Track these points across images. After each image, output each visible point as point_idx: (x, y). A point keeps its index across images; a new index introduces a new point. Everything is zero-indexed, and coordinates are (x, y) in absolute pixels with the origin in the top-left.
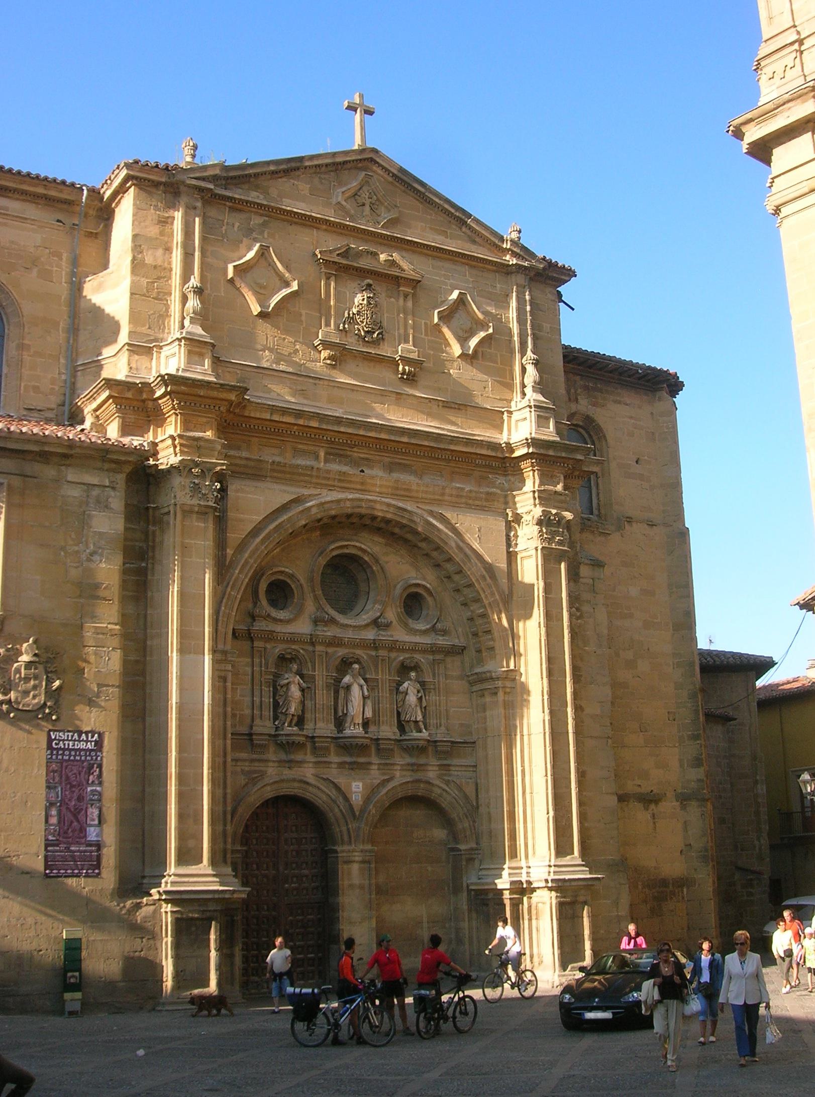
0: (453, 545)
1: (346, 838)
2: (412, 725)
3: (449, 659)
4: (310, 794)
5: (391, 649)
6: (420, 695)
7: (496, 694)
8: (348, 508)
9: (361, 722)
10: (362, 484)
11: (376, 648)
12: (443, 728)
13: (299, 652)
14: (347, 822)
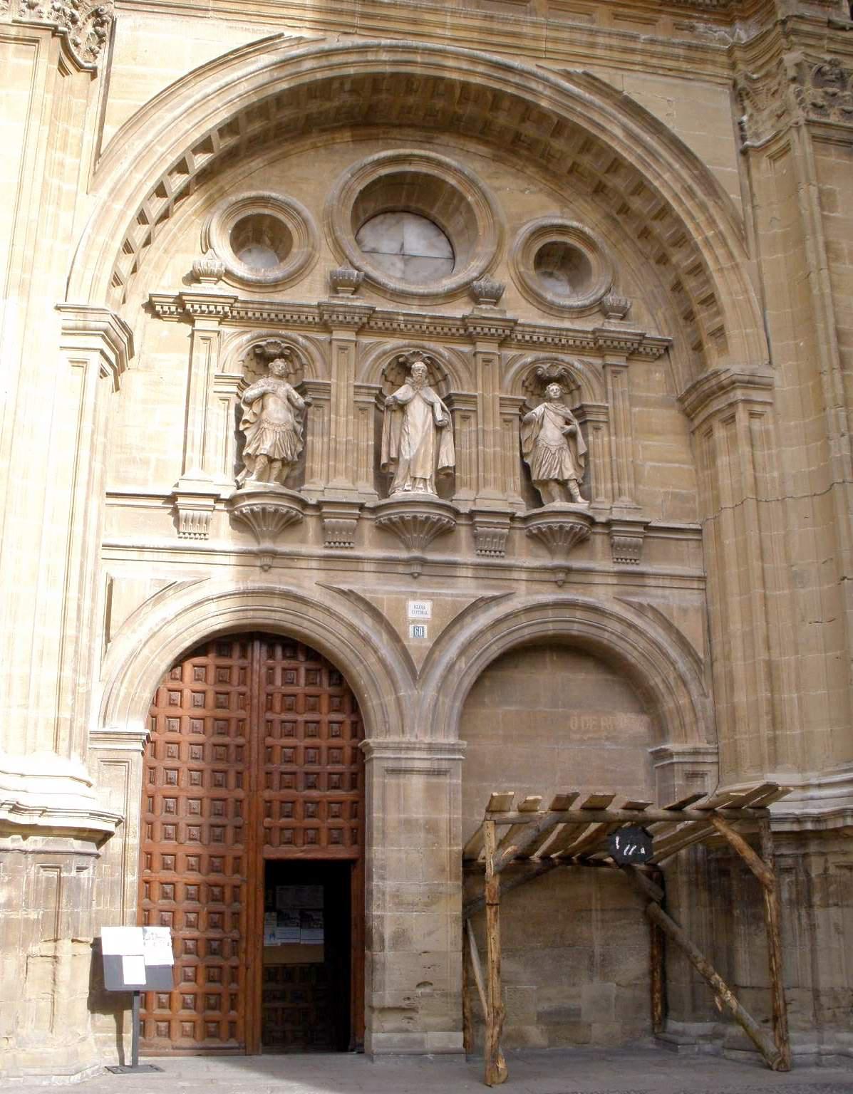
0: (619, 132)
1: (393, 719)
2: (555, 489)
3: (638, 368)
4: (309, 625)
5: (504, 342)
6: (568, 428)
7: (733, 417)
8: (383, 63)
9: (428, 471)
10: (415, 22)
11: (471, 339)
12: (625, 500)
13: (296, 341)
14: (393, 683)
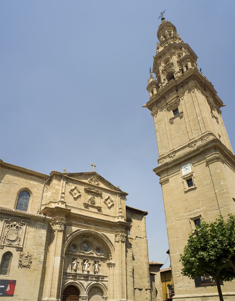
1: (83, 294)
